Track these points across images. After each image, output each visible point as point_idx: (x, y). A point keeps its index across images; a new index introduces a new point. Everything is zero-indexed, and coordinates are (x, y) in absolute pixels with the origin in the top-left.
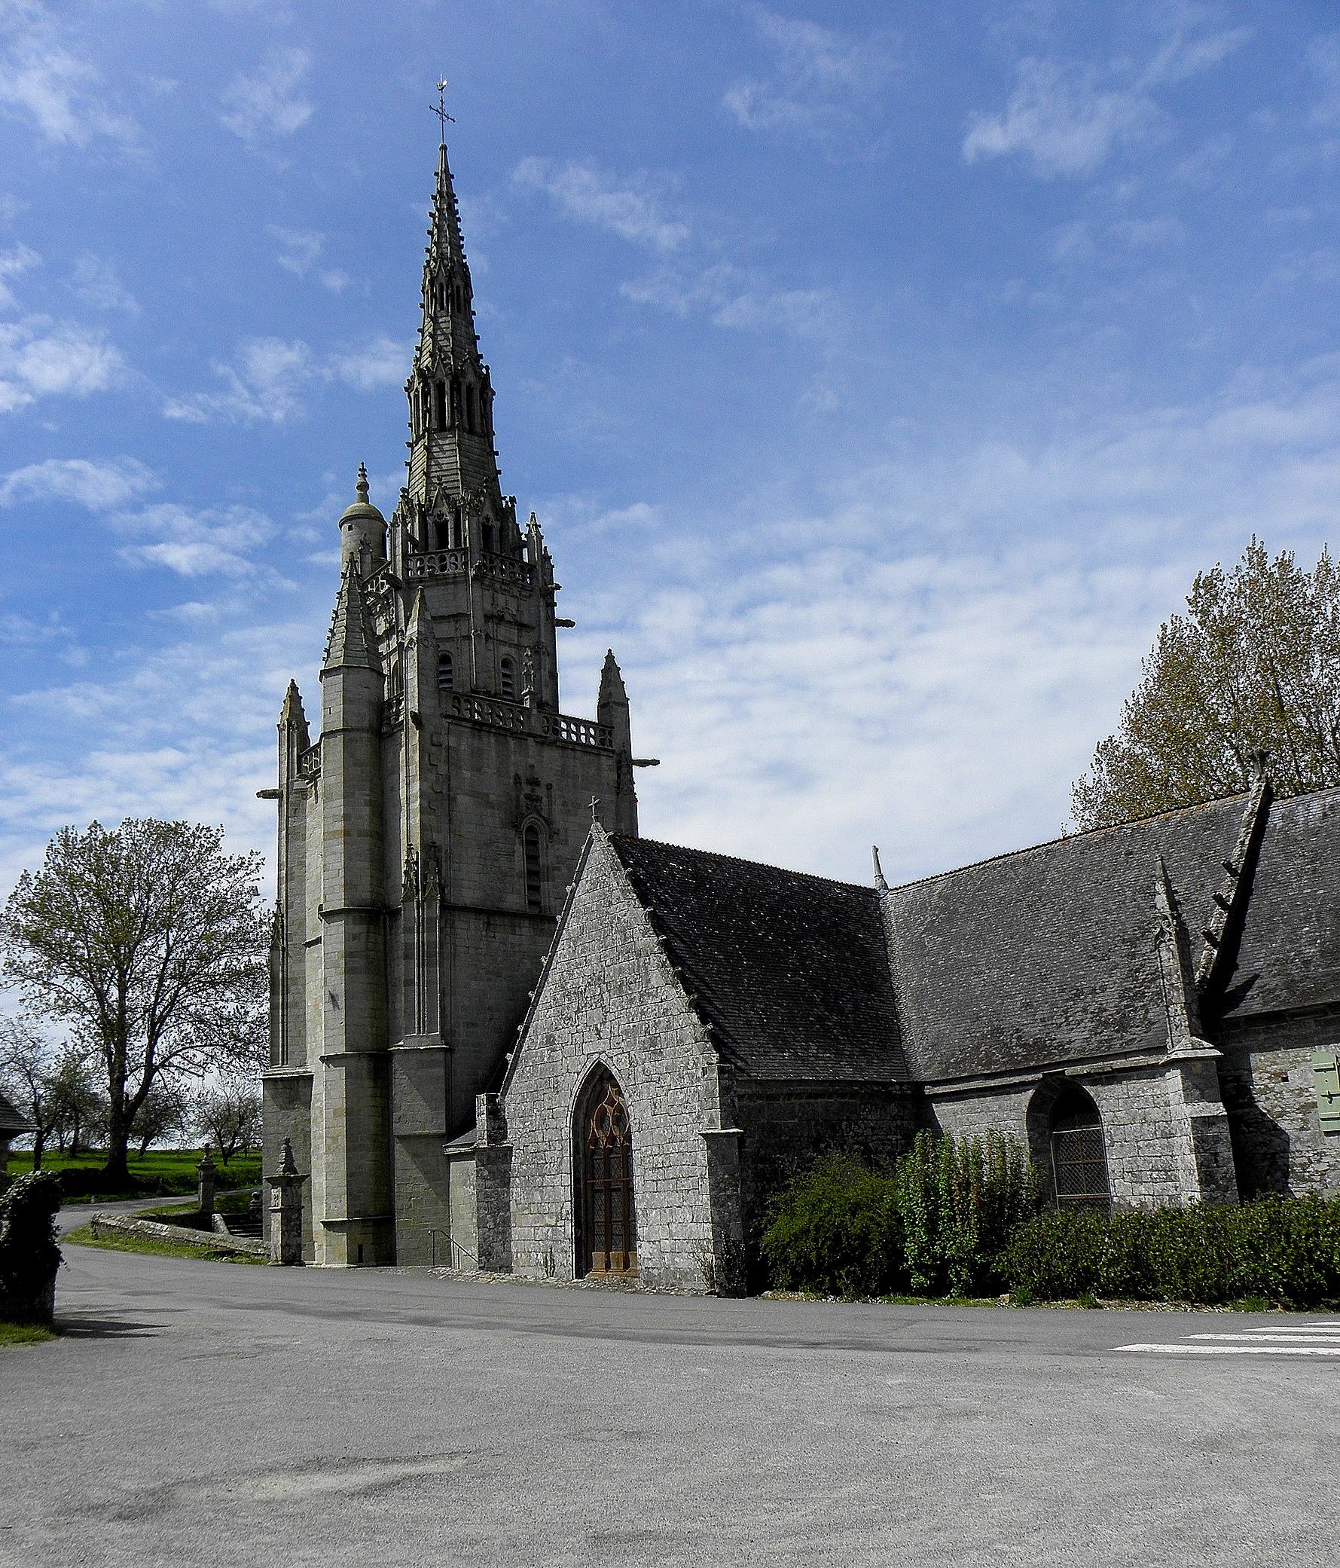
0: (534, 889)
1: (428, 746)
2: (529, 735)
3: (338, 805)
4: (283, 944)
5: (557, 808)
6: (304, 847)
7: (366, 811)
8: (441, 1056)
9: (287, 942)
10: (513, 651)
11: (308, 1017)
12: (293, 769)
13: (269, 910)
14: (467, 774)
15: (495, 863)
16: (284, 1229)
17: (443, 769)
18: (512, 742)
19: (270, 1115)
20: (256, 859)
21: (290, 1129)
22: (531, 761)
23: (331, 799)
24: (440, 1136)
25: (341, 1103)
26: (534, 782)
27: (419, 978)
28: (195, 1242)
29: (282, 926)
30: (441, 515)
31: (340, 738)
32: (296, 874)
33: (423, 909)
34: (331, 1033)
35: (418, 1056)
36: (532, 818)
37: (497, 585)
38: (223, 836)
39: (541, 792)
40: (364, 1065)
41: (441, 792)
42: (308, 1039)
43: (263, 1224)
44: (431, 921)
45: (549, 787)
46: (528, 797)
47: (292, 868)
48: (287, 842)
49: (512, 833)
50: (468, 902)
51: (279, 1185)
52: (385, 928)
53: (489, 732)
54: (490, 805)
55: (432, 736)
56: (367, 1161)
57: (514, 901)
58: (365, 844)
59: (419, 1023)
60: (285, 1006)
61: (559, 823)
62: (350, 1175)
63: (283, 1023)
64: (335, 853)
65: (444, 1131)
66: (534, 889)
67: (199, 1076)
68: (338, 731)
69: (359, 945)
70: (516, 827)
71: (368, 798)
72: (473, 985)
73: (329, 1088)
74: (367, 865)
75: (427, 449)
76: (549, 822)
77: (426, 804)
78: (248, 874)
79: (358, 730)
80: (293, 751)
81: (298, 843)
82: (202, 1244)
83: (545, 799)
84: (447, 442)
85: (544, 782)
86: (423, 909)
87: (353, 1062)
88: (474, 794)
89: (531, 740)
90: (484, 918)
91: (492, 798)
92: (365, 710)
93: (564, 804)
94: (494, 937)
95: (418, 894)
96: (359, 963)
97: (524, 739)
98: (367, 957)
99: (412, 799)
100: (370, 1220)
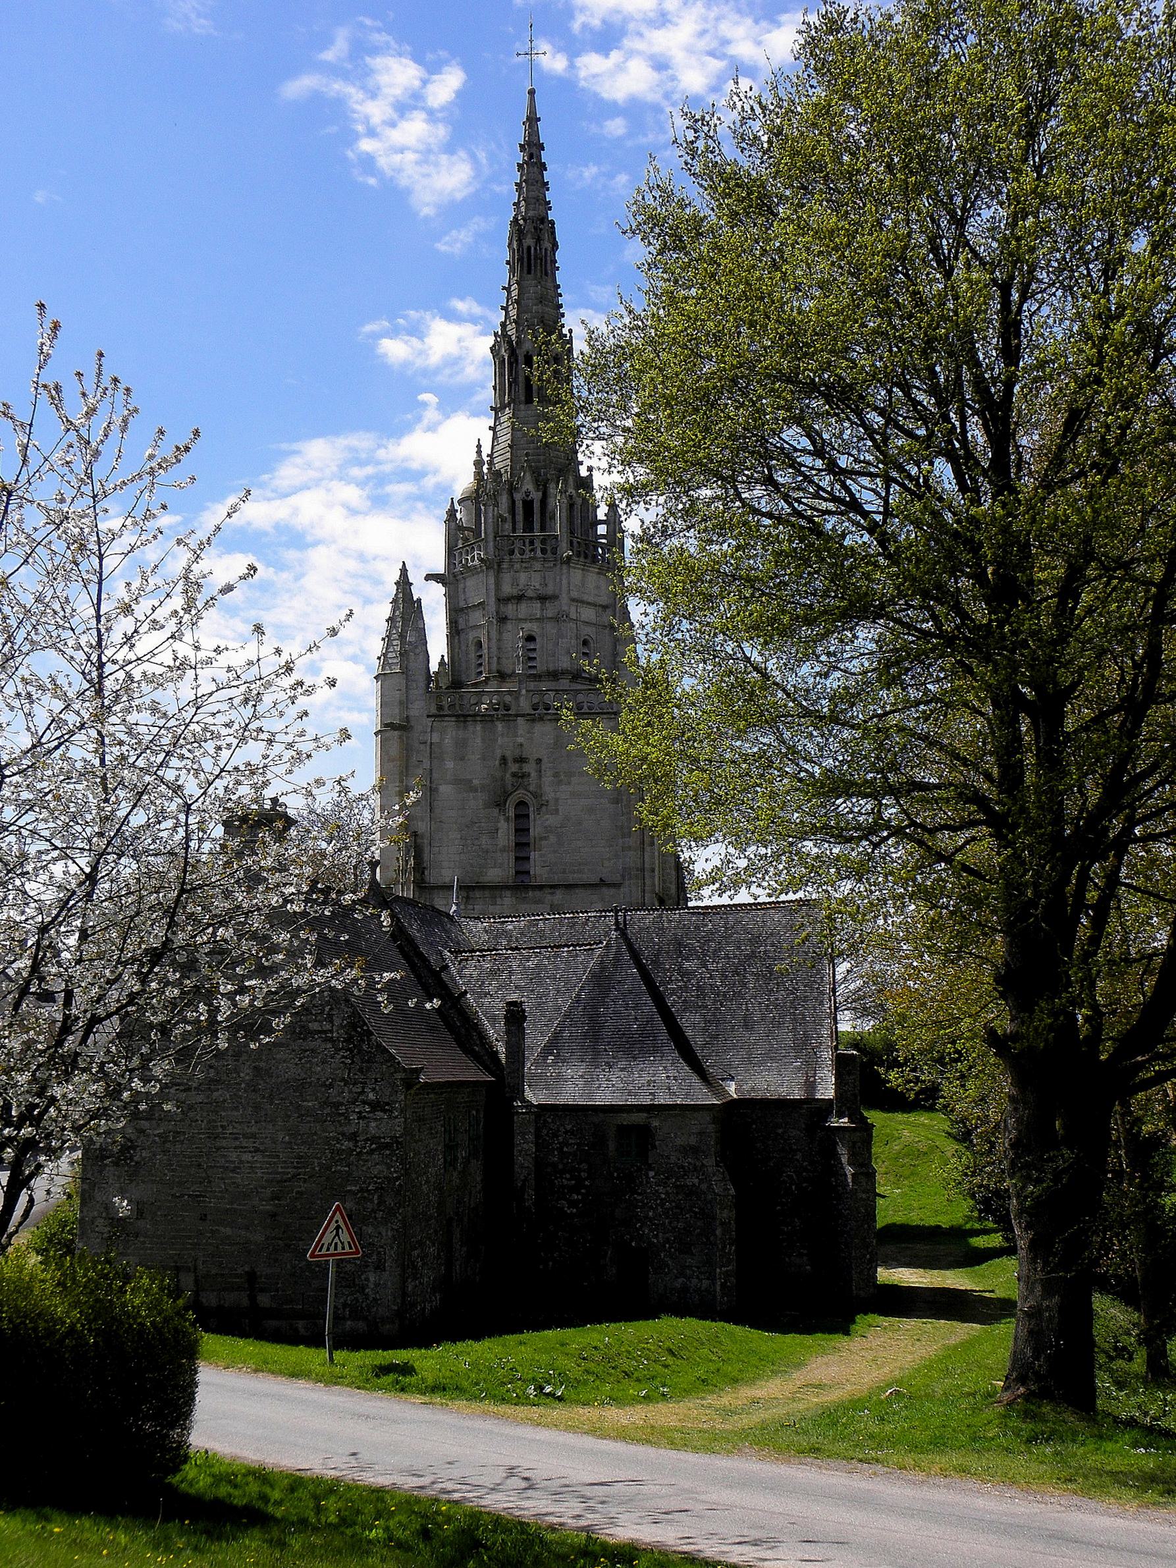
0: (522, 859)
2: (517, 716)
5: (547, 779)
14: (450, 765)
15: (476, 842)
22: (520, 740)
26: (521, 760)
39: (529, 768)
45: (539, 761)
54: (474, 790)
66: (522, 859)
70: (500, 804)
76: (536, 795)
83: (533, 774)
88: (457, 781)
91: (476, 782)
93: (556, 775)
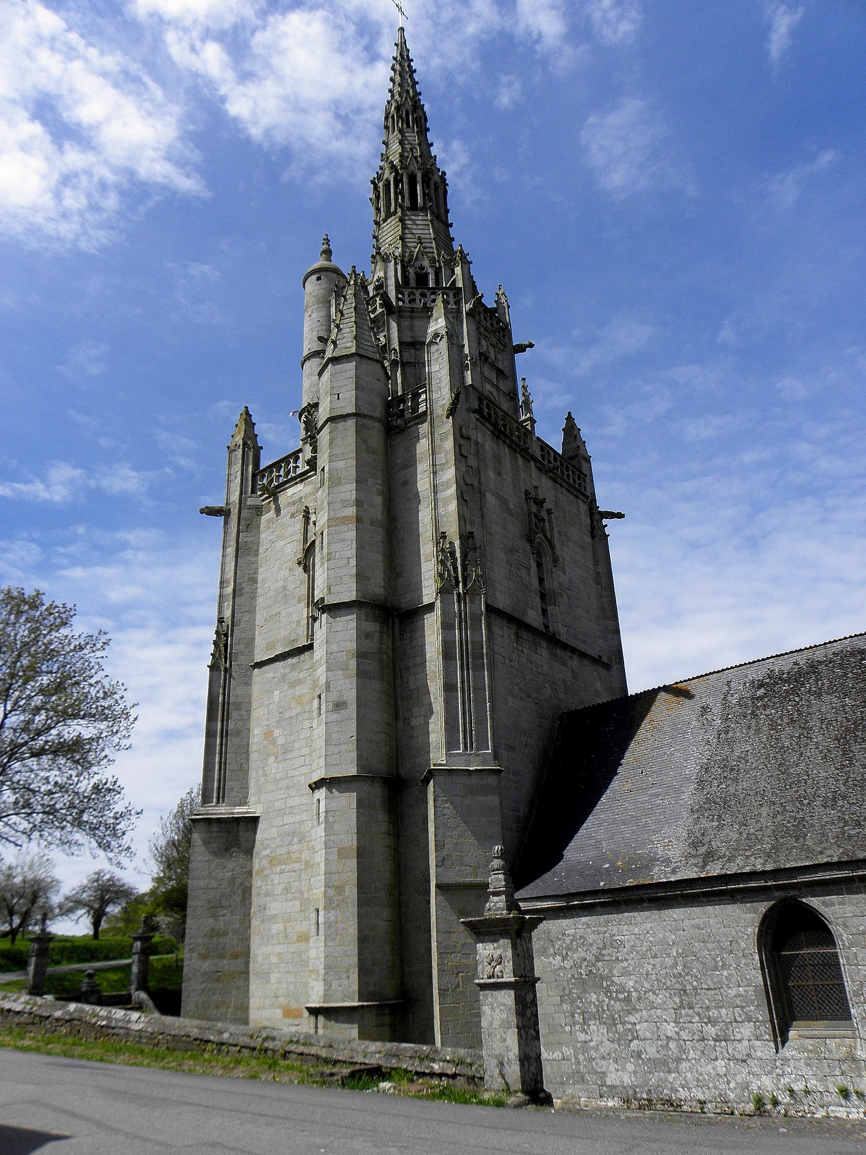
3: (349, 490)
4: (226, 663)
5: (556, 535)
6: (256, 562)
7: (379, 500)
9: (231, 663)
10: (494, 392)
11: (253, 747)
12: (246, 487)
13: (118, 682)
14: (492, 474)
16: (521, 1025)
17: (473, 462)
18: (520, 460)
19: (200, 865)
20: (103, 639)
21: (225, 884)
22: (535, 483)
25: (351, 841)
26: (540, 503)
27: (463, 682)
28: (222, 1044)
29: (226, 646)
30: (422, 268)
31: (351, 423)
32: (246, 590)
33: (465, 603)
34: (336, 749)
35: (465, 779)
37: (482, 329)
38: (75, 614)
39: (544, 514)
40: (378, 790)
41: (472, 485)
42: (252, 773)
44: (475, 619)
45: (549, 512)
46: (536, 516)
47: (240, 585)
48: (237, 557)
49: (527, 546)
50: (501, 606)
51: (503, 934)
52: (393, 633)
53: (504, 442)
54: (509, 511)
56: (382, 922)
57: (533, 617)
58: (378, 535)
59: (465, 738)
60: (225, 734)
61: (558, 552)
62: (363, 940)
63: (221, 754)
66: (544, 612)
67: (17, 845)
68: (348, 416)
69: (373, 645)
70: (530, 541)
71: (380, 487)
72: (510, 700)
73: (331, 819)
74: (380, 558)
75: (401, 220)
76: (552, 547)
78: (94, 652)
79: (370, 417)
80: (247, 469)
81: (250, 558)
82: (242, 1047)
83: (547, 523)
84: (420, 218)
86: (465, 603)
87: (365, 787)
88: (499, 497)
89: (532, 463)
91: (511, 506)
92: (378, 401)
93: (560, 532)
95: (457, 585)
96: (372, 666)
98: (381, 661)
99: (440, 488)
100: (387, 1005)
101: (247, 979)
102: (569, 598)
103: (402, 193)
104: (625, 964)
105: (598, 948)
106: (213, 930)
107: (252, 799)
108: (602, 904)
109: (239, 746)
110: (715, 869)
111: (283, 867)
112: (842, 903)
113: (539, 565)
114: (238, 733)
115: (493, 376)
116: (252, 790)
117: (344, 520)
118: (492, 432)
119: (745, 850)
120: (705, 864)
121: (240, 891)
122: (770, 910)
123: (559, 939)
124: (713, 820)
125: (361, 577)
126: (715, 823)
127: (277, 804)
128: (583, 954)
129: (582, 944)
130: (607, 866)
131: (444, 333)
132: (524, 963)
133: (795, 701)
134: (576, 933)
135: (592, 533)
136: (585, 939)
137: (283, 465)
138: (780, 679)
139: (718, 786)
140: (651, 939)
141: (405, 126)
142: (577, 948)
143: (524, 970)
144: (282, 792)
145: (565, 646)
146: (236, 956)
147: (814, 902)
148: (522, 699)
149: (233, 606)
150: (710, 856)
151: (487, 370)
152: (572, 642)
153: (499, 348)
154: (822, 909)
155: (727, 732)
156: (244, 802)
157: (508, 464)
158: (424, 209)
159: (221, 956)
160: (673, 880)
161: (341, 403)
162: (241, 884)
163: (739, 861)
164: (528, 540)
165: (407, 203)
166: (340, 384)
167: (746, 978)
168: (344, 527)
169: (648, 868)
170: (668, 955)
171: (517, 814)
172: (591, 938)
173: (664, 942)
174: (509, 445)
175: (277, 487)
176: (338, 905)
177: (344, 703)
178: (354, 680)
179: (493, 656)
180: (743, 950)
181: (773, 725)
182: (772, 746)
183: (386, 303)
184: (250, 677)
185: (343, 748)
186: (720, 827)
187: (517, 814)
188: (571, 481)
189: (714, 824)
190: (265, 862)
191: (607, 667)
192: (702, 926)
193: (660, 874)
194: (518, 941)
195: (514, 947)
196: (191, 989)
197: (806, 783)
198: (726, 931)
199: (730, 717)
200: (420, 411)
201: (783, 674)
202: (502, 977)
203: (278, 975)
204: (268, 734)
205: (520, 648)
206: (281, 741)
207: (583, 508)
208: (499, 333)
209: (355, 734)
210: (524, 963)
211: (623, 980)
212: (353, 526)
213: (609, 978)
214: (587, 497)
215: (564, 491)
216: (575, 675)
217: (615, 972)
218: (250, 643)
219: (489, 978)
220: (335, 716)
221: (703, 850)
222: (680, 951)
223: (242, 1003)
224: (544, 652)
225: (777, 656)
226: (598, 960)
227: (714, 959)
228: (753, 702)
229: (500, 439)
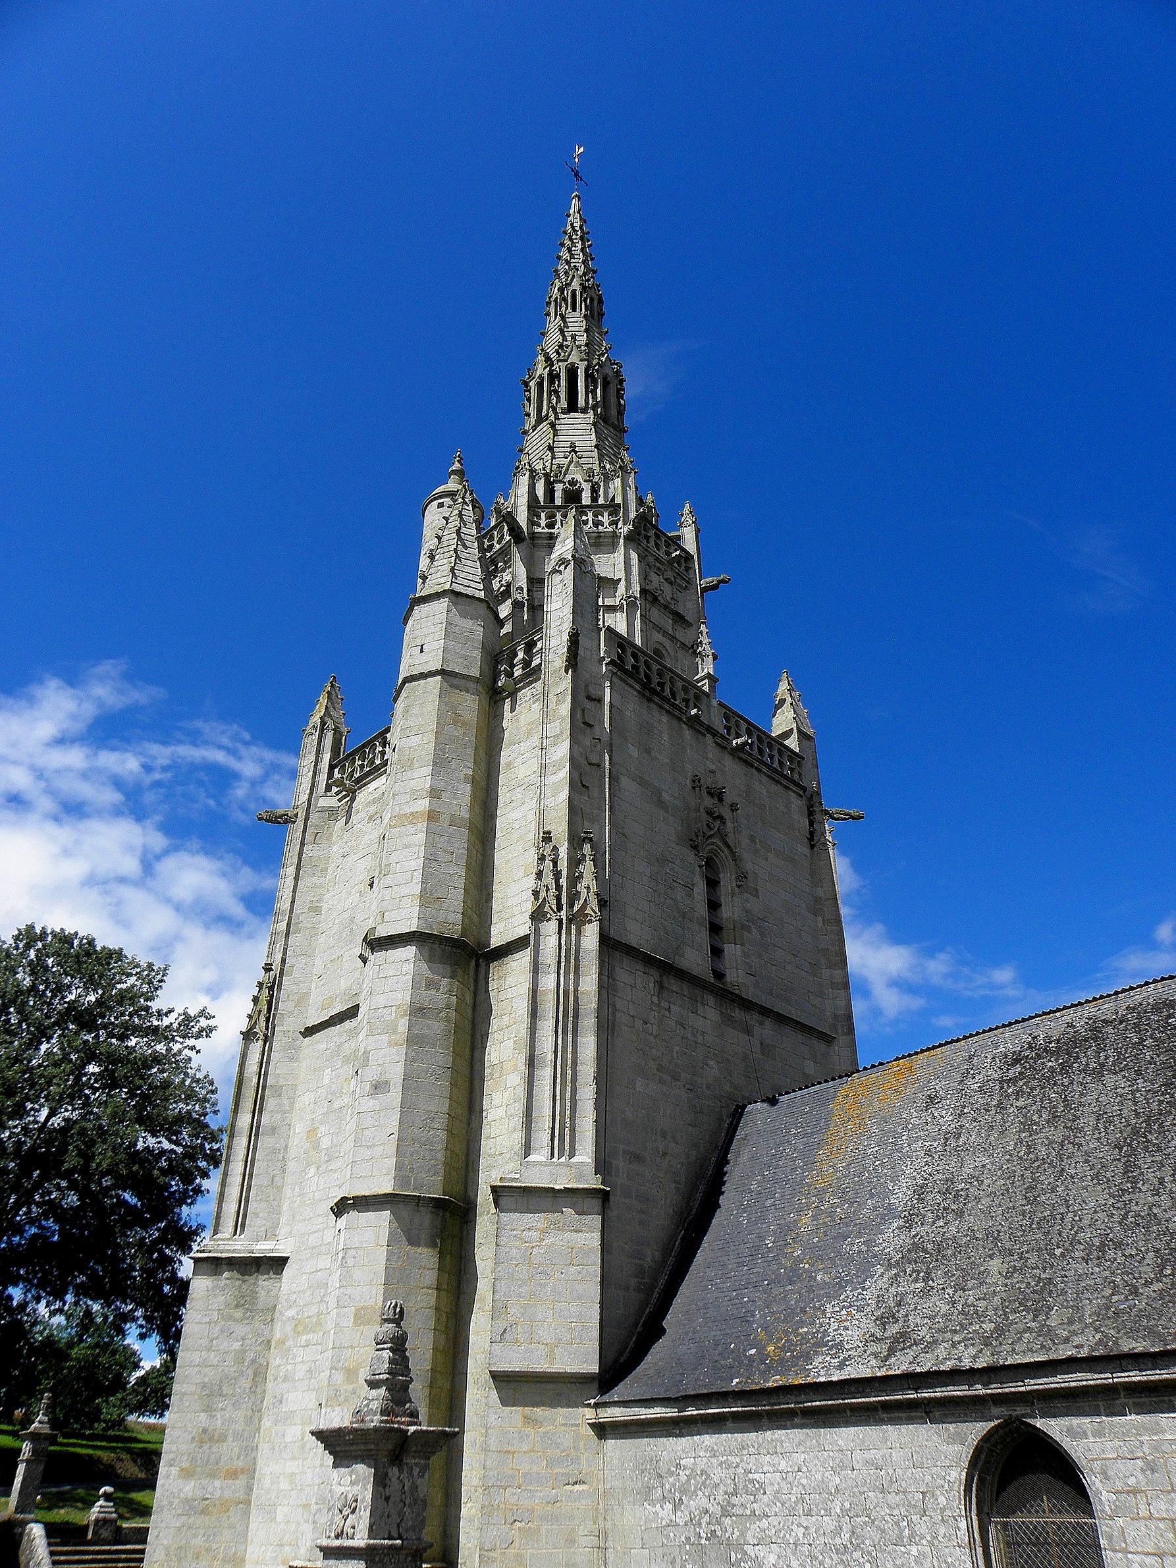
0: (717, 952)
1: (582, 697)
5: (745, 842)
7: (466, 791)
8: (596, 1203)
10: (667, 643)
11: (292, 1153)
14: (634, 752)
15: (670, 892)
21: (230, 1360)
23: (411, 767)
24: (579, 1380)
26: (717, 795)
32: (305, 924)
34: (368, 1153)
36: (712, 844)
37: (651, 559)
40: (426, 1220)
42: (288, 1192)
43: (148, 1548)
45: (734, 808)
48: (296, 879)
49: (690, 856)
54: (661, 804)
55: (587, 686)
57: (695, 960)
64: (407, 846)
65: (593, 1367)
66: (717, 952)
68: (431, 674)
72: (639, 1084)
73: (350, 1262)
74: (462, 872)
77: (576, 776)
85: (729, 797)
88: (641, 782)
90: (655, 973)
91: (665, 796)
93: (752, 839)
94: (669, 1010)
95: (560, 908)
96: (436, 1027)
97: (701, 733)
101: (247, 1514)
102: (762, 934)
103: (556, 392)
104: (764, 1523)
105: (726, 1493)
106: (205, 1431)
107: (283, 1231)
108: (735, 1417)
109: (274, 1151)
110: (900, 1365)
111: (310, 1336)
112: (1099, 1433)
113: (712, 884)
114: (273, 1130)
115: (668, 623)
116: (284, 1218)
117: (412, 818)
118: (639, 692)
119: (955, 1332)
120: (891, 1352)
121: (250, 1372)
122: (987, 1438)
123: (671, 1474)
124: (916, 1280)
125: (427, 898)
126: (920, 1285)
127: (311, 1238)
128: (704, 1502)
129: (704, 1483)
130: (753, 1351)
131: (570, 558)
132: (401, 1514)
133: (1062, 1084)
134: (695, 1464)
135: (811, 839)
136: (708, 1476)
137: (367, 750)
138: (1045, 1050)
139: (934, 1223)
140: (804, 1481)
141: (570, 309)
142: (695, 1491)
143: (398, 1526)
144: (320, 1220)
145: (747, 1005)
146: (233, 1474)
147: (1054, 1427)
148: (662, 1082)
149: (285, 950)
150: (900, 1341)
151: (656, 614)
152: (764, 1000)
153: (679, 585)
154: (1067, 1444)
155: (958, 1136)
156: (270, 1235)
157: (666, 737)
158: (584, 411)
159: (213, 1475)
160: (834, 1379)
161: (424, 658)
162: (254, 1361)
163: (941, 1351)
164: (692, 847)
165: (564, 404)
166: (426, 631)
167: (946, 1562)
168: (411, 829)
169: (808, 1358)
170: (828, 1512)
171: (638, 1262)
172: (717, 1474)
173: (822, 1488)
174: (667, 711)
175: (358, 781)
176: (346, 1400)
177: (386, 1083)
178: (403, 1049)
179: (614, 1014)
180: (943, 1510)
181: (1027, 1125)
182: (1021, 1158)
183: (515, 530)
184: (297, 1049)
185: (378, 1151)
186: (925, 1293)
187: (638, 1262)
188: (776, 765)
189: (918, 1285)
190: (289, 1328)
191: (828, 1039)
192: (880, 1462)
193: (823, 1370)
194: (394, 1472)
195: (380, 1481)
196: (163, 1525)
197: (1062, 1219)
198: (918, 1473)
199: (965, 1111)
200: (533, 665)
201: (1050, 1043)
202: (352, 1538)
203: (286, 1509)
204: (311, 1133)
205: (665, 1004)
206: (326, 1142)
207: (797, 804)
208: (679, 564)
209: (395, 1130)
210: (401, 1514)
211: (760, 1551)
212: (423, 826)
213: (740, 1546)
214: (804, 789)
215: (764, 779)
216: (766, 1049)
217: (749, 1537)
218: (302, 1000)
219: (337, 1537)
220: (372, 1102)
221: (893, 1330)
222: (847, 1505)
223: (235, 1553)
224: (709, 1013)
225: (1044, 1014)
226: (725, 1513)
227: (897, 1524)
228: (1002, 1088)
229: (654, 702)
